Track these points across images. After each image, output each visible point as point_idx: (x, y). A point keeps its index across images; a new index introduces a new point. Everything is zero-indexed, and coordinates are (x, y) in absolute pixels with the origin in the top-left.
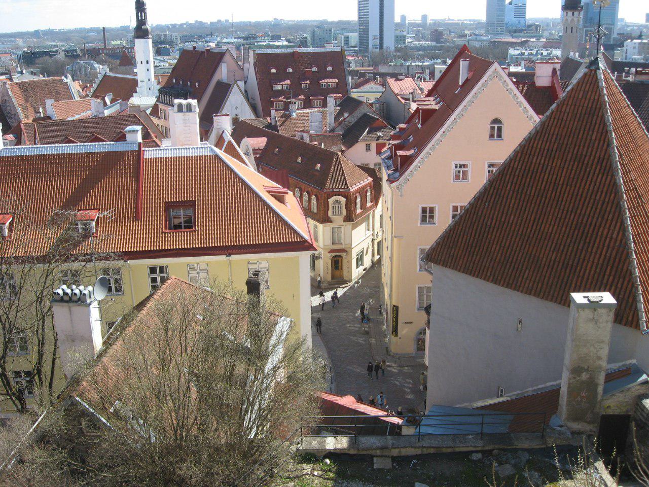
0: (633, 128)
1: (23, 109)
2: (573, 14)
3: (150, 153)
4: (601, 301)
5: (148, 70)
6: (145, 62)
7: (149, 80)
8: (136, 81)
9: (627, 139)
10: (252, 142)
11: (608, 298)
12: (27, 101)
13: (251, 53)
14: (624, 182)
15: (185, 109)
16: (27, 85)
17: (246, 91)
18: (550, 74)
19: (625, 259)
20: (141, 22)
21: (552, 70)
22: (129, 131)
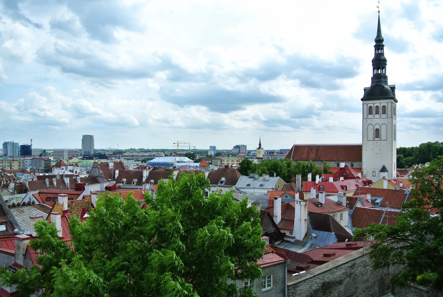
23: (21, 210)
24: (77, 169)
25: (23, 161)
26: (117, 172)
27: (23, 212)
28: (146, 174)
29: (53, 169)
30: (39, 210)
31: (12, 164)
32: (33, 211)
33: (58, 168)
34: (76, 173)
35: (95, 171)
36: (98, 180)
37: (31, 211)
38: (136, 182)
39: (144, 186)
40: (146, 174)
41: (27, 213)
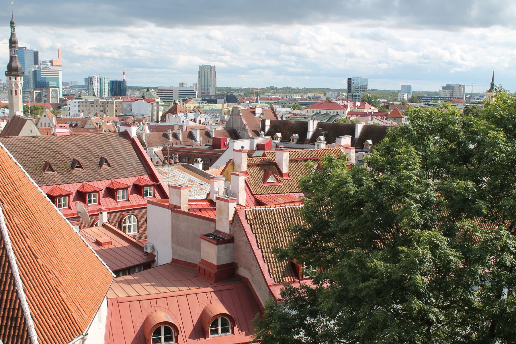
0: (14, 177)
2: (16, 79)
9: (10, 189)
14: (8, 228)
23: (162, 171)
24: (201, 117)
25: (121, 104)
26: (268, 123)
27: (166, 173)
28: (312, 127)
29: (167, 114)
30: (185, 173)
31: (107, 109)
32: (177, 173)
33: (174, 116)
34: (200, 123)
35: (236, 121)
36: (240, 134)
37: (174, 172)
38: (297, 139)
39: (316, 145)
40: (312, 127)
41: (170, 175)
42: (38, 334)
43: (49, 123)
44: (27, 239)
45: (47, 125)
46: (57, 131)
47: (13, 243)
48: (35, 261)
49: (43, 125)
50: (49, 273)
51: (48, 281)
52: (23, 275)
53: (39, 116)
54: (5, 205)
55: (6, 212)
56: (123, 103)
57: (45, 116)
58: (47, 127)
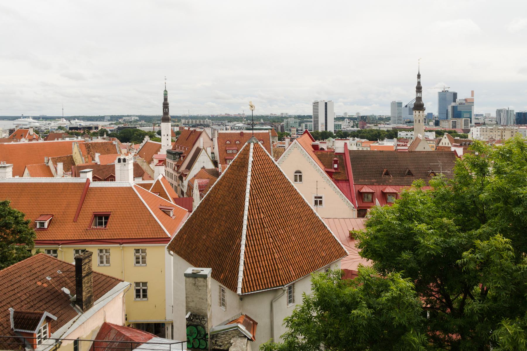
1: (85, 158)
3: (94, 184)
4: (200, 272)
5: (167, 140)
6: (166, 135)
7: (168, 145)
8: (161, 145)
10: (199, 182)
11: (207, 271)
12: (89, 153)
13: (216, 132)
15: (122, 161)
16: (90, 145)
17: (213, 153)
18: (343, 146)
19: (239, 250)
20: (166, 113)
21: (344, 144)
22: (82, 172)
42: (244, 276)
43: (448, 143)
44: (262, 214)
45: (447, 144)
46: (398, 148)
47: (250, 215)
48: (263, 229)
49: (444, 144)
50: (271, 239)
51: (268, 243)
52: (249, 236)
53: (441, 137)
54: (254, 191)
55: (253, 195)
56: (519, 130)
57: (445, 138)
58: (447, 145)
